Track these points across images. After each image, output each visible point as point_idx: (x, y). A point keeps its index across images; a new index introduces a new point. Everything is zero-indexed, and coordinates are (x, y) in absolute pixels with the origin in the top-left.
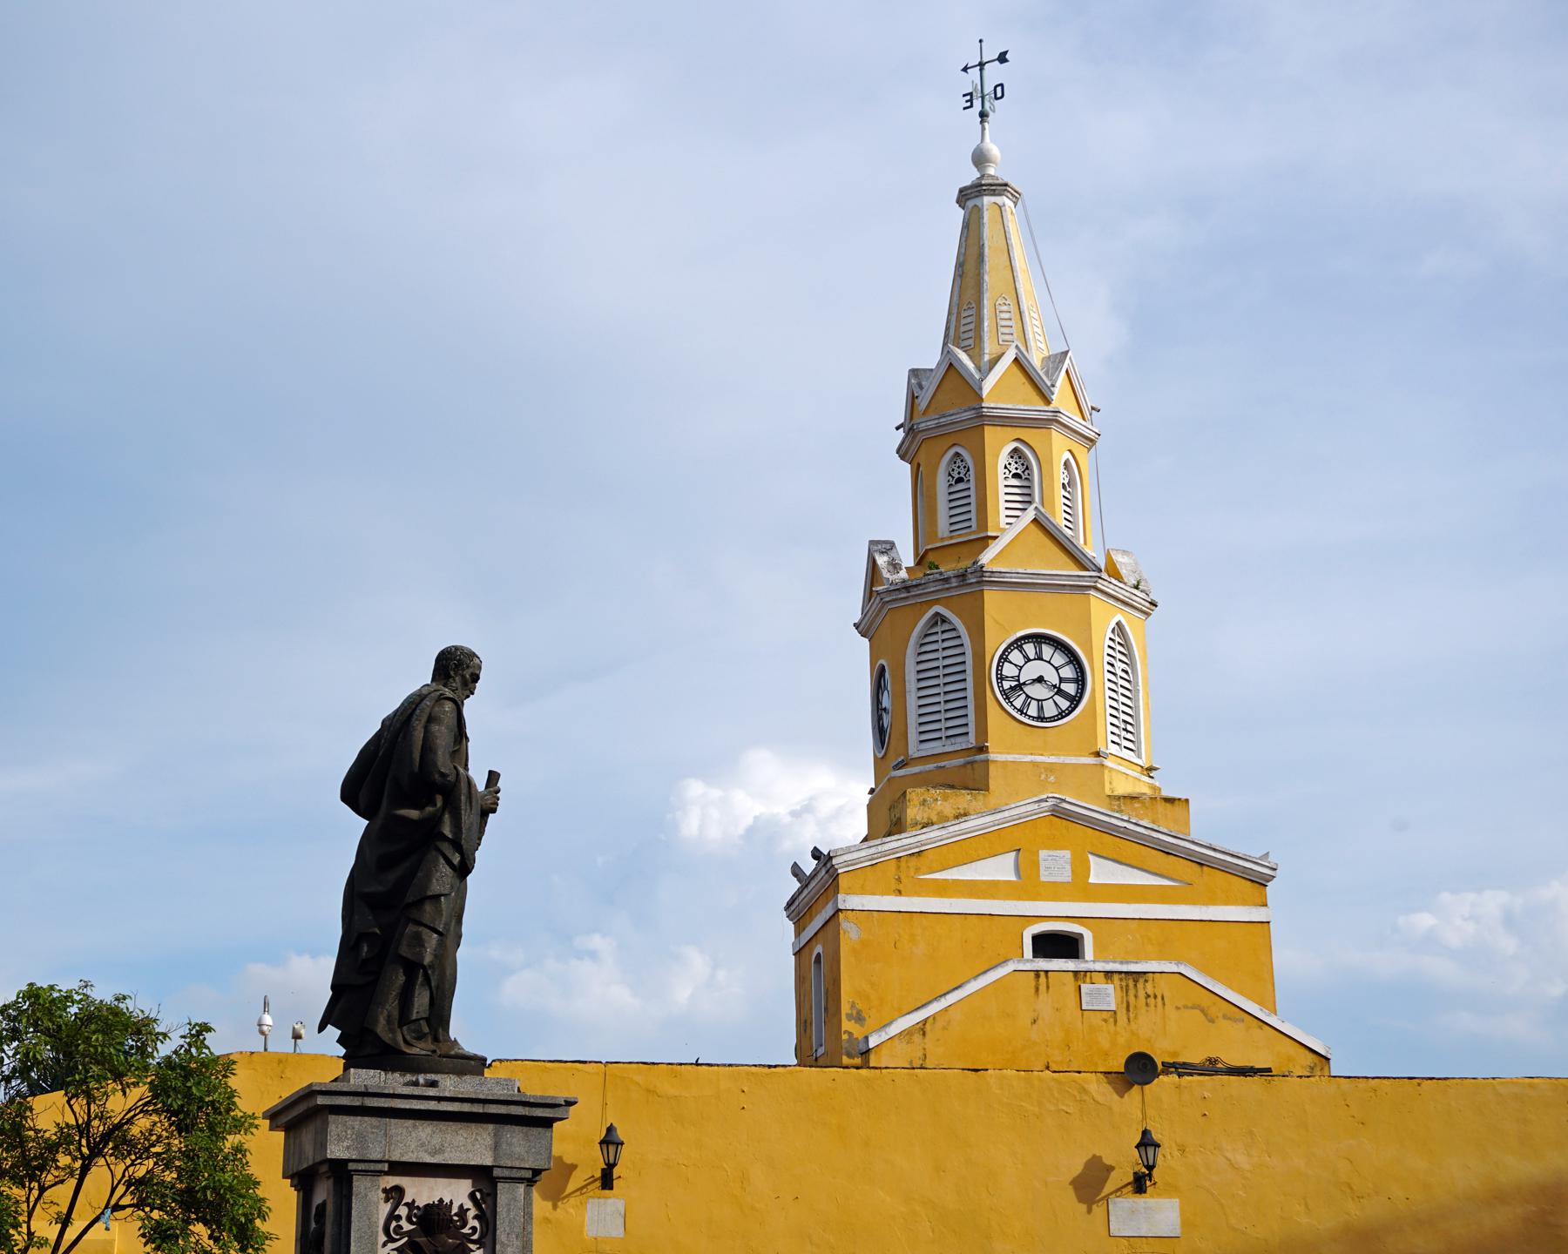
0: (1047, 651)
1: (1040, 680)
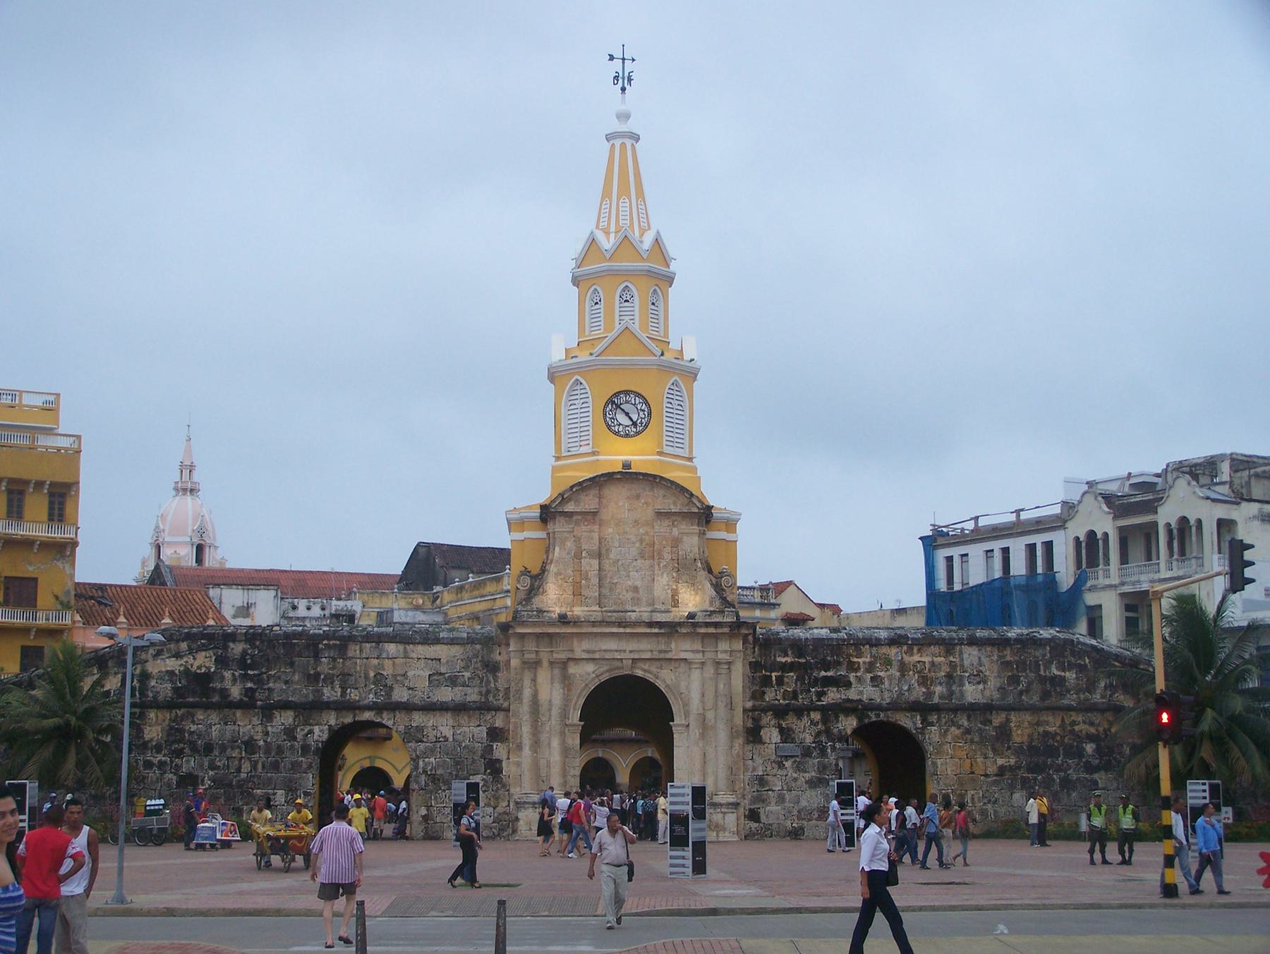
0: (632, 398)
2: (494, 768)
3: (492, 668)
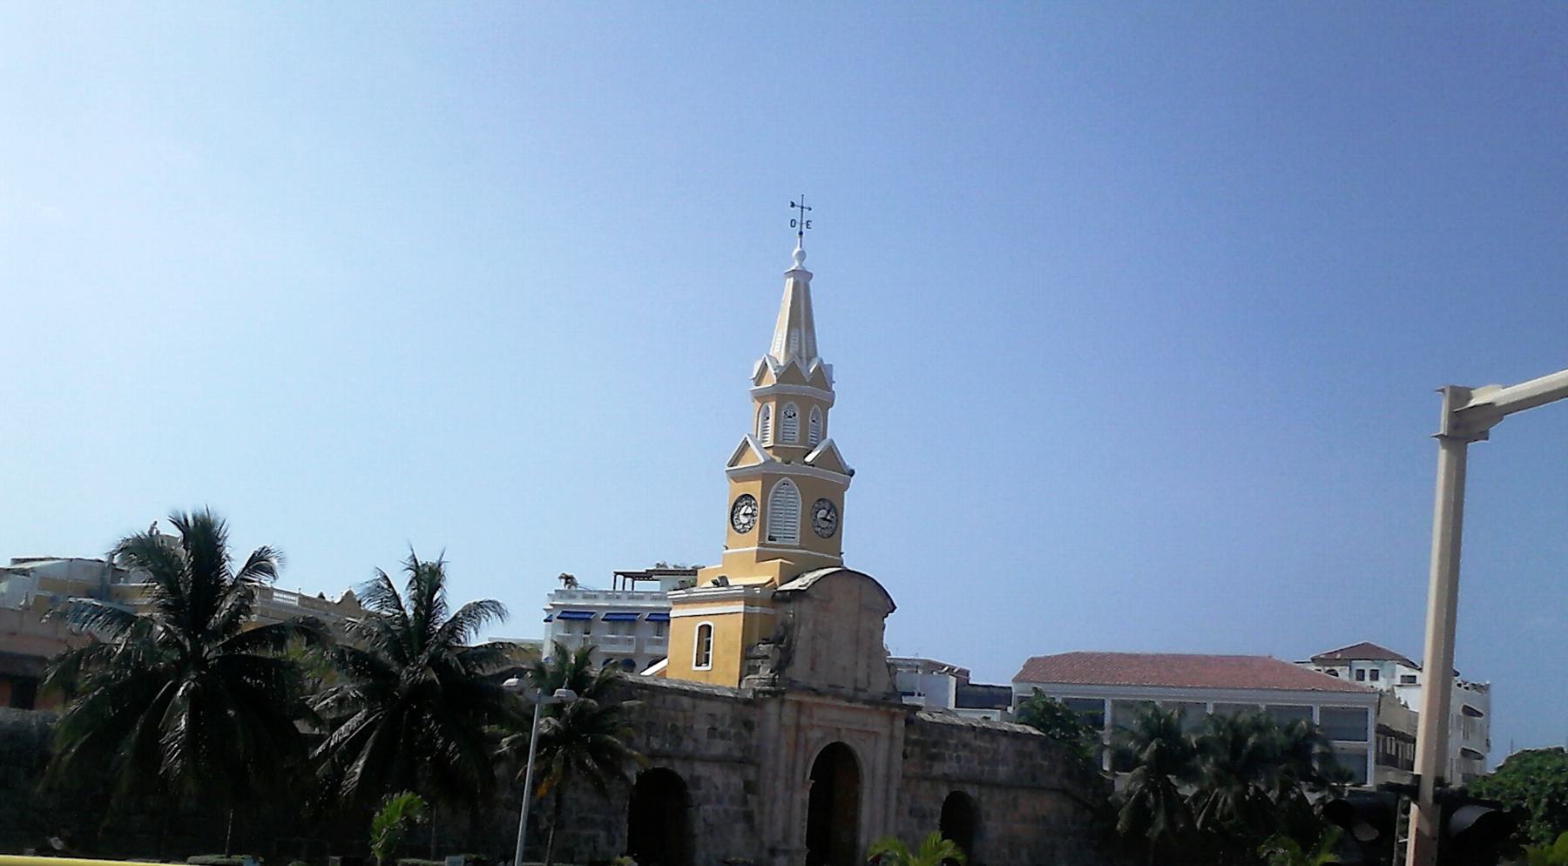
2: (748, 817)
3: (749, 725)
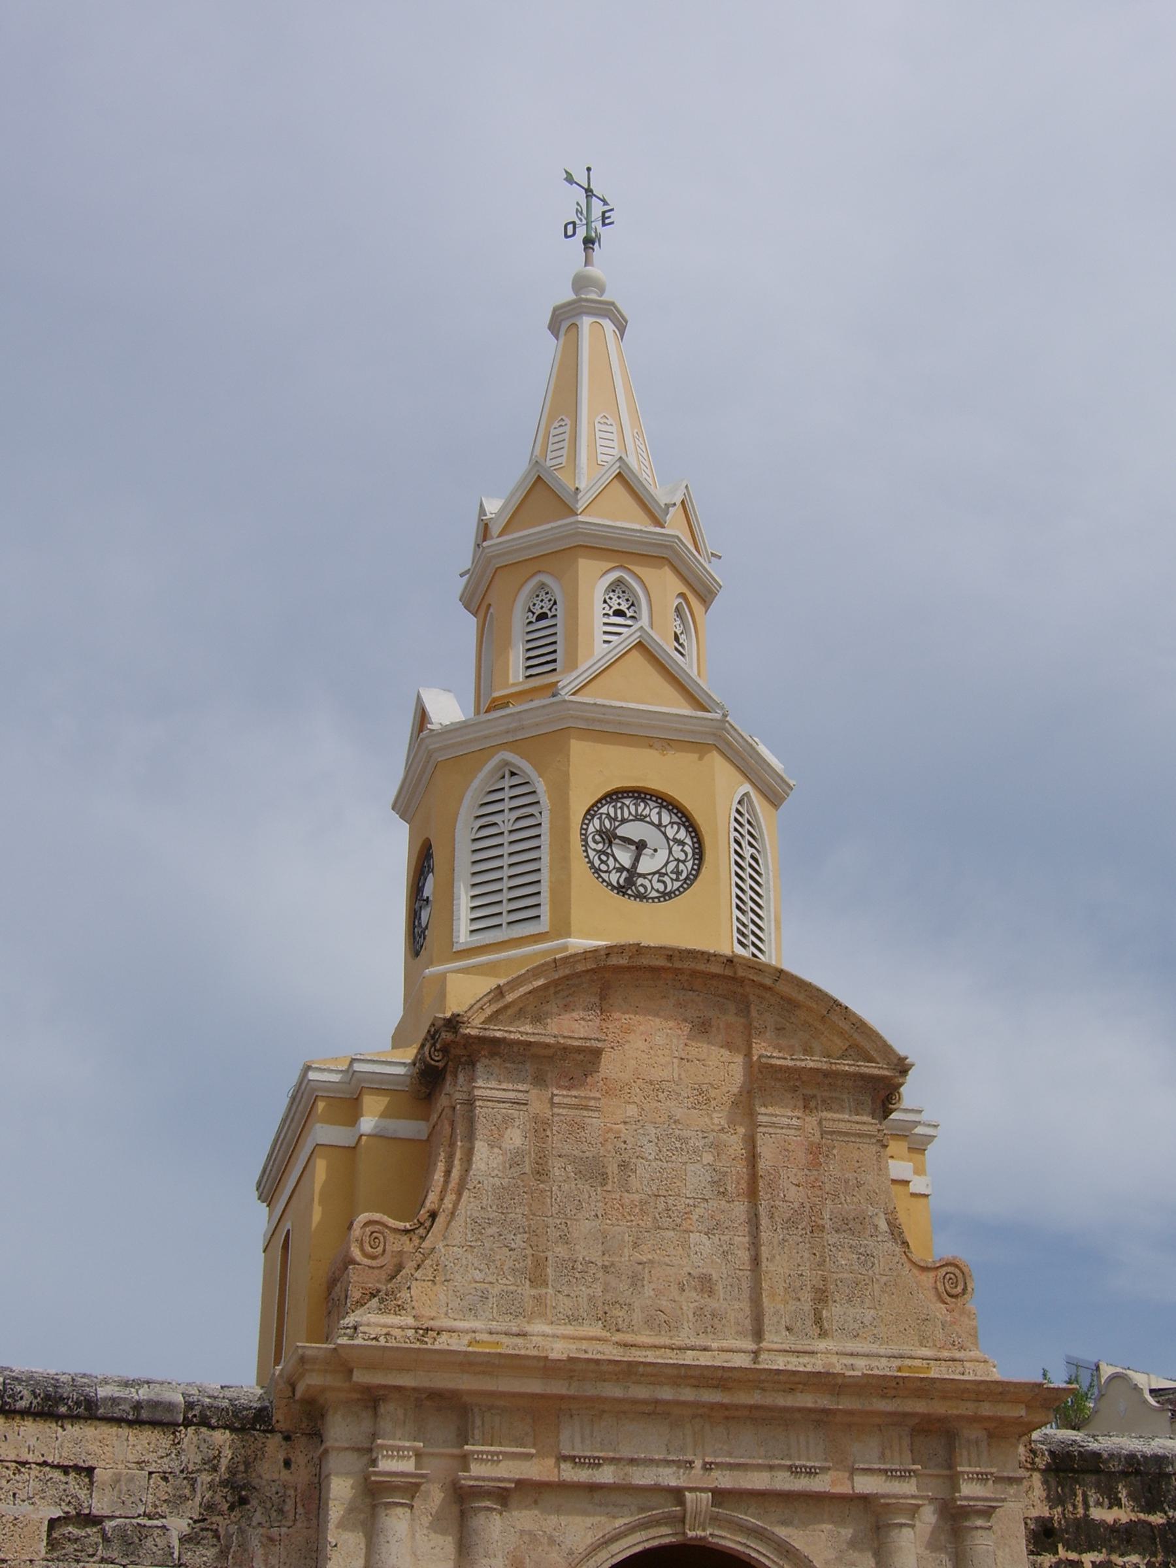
1: (641, 846)
